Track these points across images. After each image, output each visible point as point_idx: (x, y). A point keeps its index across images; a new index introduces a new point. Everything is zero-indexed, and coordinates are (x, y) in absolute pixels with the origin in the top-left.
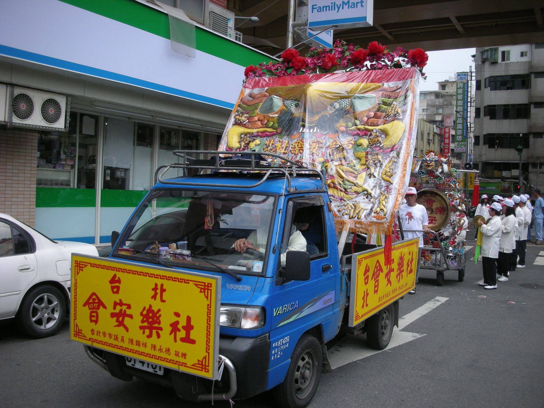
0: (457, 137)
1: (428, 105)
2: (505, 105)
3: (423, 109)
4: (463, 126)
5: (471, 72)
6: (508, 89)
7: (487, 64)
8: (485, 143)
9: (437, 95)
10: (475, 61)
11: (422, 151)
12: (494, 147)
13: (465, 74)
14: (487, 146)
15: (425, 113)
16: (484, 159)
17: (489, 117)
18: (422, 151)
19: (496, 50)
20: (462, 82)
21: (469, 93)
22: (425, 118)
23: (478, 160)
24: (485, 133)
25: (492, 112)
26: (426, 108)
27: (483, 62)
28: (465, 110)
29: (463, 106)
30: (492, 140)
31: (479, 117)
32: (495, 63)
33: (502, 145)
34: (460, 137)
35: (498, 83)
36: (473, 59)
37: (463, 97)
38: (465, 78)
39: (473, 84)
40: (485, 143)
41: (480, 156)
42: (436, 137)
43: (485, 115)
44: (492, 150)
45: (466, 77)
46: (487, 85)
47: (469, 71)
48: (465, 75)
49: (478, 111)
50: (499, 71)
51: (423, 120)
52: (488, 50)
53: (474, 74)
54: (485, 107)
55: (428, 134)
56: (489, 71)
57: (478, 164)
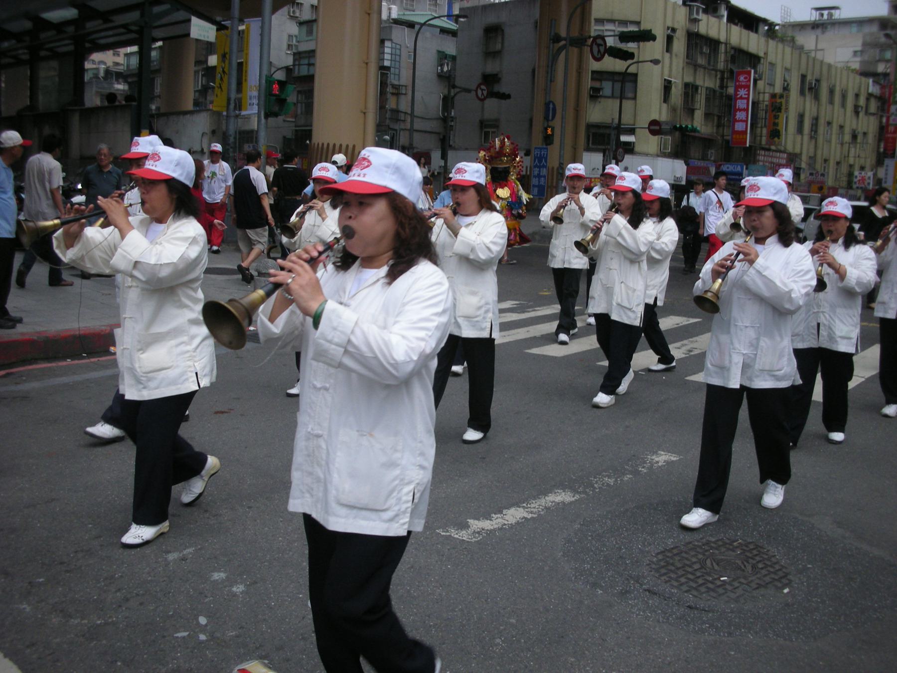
1: (865, 44)
3: (855, 52)
11: (841, 127)
15: (858, 59)
26: (859, 48)
51: (854, 71)
55: (857, 96)
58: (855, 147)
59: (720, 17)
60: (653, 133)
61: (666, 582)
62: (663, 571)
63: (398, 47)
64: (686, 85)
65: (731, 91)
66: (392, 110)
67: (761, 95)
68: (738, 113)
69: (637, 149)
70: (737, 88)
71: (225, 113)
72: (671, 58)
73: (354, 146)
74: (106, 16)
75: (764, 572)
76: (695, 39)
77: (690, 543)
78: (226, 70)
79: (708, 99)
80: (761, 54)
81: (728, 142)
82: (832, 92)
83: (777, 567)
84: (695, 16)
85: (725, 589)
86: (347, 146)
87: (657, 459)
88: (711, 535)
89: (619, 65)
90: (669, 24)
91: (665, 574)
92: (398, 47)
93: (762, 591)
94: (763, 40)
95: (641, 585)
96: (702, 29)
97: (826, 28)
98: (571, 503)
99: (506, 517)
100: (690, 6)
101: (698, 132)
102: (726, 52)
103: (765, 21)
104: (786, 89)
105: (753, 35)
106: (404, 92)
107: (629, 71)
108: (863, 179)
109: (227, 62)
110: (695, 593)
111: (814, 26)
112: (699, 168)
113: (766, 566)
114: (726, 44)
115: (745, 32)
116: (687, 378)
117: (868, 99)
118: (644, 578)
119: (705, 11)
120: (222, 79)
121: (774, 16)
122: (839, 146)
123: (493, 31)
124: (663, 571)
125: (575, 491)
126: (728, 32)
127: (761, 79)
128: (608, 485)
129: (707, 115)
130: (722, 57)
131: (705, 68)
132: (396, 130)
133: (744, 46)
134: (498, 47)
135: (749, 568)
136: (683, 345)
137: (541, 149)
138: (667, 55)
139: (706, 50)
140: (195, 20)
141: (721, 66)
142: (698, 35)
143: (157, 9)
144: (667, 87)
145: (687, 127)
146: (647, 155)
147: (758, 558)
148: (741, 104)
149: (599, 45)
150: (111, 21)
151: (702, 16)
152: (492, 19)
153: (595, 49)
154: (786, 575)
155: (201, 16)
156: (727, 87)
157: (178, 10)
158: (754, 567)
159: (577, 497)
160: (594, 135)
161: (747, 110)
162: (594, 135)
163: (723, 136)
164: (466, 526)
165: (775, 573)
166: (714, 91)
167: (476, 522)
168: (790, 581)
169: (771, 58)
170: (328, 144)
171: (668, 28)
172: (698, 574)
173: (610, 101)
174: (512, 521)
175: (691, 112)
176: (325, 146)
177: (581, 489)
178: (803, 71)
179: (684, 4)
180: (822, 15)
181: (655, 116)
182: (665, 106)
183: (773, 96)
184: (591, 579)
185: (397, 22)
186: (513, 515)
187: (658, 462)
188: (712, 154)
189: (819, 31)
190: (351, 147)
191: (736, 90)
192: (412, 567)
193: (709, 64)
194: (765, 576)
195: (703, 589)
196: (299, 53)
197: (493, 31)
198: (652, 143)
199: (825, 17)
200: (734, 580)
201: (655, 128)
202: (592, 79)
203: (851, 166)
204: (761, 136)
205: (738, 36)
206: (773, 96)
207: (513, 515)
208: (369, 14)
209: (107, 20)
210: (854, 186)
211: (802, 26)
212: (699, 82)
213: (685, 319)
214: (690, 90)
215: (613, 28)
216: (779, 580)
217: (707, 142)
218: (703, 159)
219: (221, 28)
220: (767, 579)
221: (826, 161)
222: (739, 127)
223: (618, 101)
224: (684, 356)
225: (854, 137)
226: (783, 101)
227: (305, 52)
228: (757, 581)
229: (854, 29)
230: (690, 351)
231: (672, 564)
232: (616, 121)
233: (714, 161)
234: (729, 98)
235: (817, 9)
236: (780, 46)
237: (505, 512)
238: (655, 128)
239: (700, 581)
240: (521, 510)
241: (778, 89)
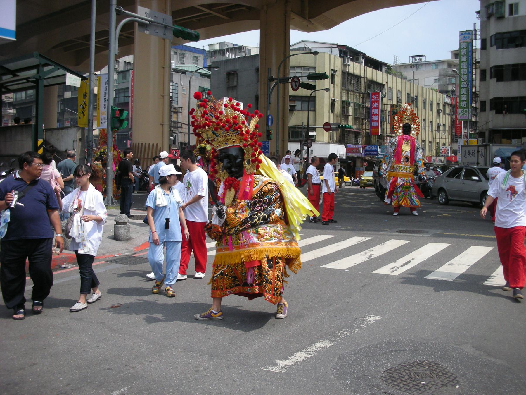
0: (462, 103)
1: (440, 75)
2: (513, 65)
3: (435, 80)
4: (468, 90)
5: (476, 31)
6: (517, 46)
7: (493, 20)
8: (491, 109)
9: (450, 64)
10: (480, 17)
11: (431, 122)
12: (502, 113)
13: (469, 32)
14: (494, 111)
15: (437, 84)
16: (491, 126)
17: (495, 79)
18: (431, 122)
19: (503, 3)
20: (465, 42)
21: (474, 54)
22: (437, 88)
23: (484, 129)
24: (492, 97)
25: (499, 73)
26: (438, 78)
27: (489, 17)
28: (470, 73)
29: (468, 68)
30: (500, 105)
31: (485, 80)
32: (501, 17)
33: (510, 111)
34: (465, 103)
35: (506, 40)
36: (478, 15)
37: (468, 58)
38: (469, 37)
39: (477, 44)
40: (491, 109)
41: (487, 123)
42: (447, 106)
43: (491, 78)
44: (500, 116)
45: (470, 36)
46: (493, 43)
47: (473, 30)
48: (469, 34)
49: (483, 73)
50: (507, 26)
52: (493, 4)
53: (478, 33)
54: (491, 68)
55: (438, 104)
56: (495, 28)
57: (484, 133)
58: (439, 133)
59: (360, 63)
60: (326, 130)
61: (393, 387)
62: (389, 381)
63: (177, 85)
64: (343, 102)
65: (368, 105)
66: (174, 122)
67: (386, 106)
68: (373, 116)
69: (317, 139)
70: (372, 103)
71: (87, 128)
72: (334, 87)
73: (157, 144)
74: (14, 73)
75: (443, 377)
76: (346, 75)
77: (400, 364)
78: (87, 103)
79: (356, 110)
80: (384, 83)
81: (368, 133)
82: (424, 103)
83: (449, 374)
84: (346, 63)
85: (425, 388)
86: (153, 144)
87: (369, 319)
88: (410, 360)
89: (305, 92)
90: (332, 68)
91: (391, 383)
92: (177, 85)
93: (445, 388)
94: (385, 75)
95: (380, 390)
96: (351, 70)
97: (419, 67)
98: (330, 347)
99: (297, 358)
100: (343, 57)
101: (352, 128)
102: (365, 82)
103: (385, 64)
104: (399, 101)
105: (379, 72)
106: (180, 110)
107: (312, 95)
108: (445, 150)
109: (87, 98)
110: (410, 392)
111: (412, 66)
112: (353, 149)
113: (444, 374)
114: (364, 78)
115: (375, 71)
116: (373, 272)
117: (444, 106)
118: (381, 386)
119: (352, 60)
120: (83, 108)
121: (390, 62)
122: (430, 133)
123: (231, 75)
124: (389, 381)
125: (330, 341)
126: (366, 71)
127: (385, 97)
128: (347, 336)
129: (356, 119)
130: (362, 85)
131: (353, 92)
132: (177, 133)
133: (375, 79)
134: (235, 83)
135: (435, 376)
136: (366, 253)
137: (265, 142)
138: (332, 85)
139: (353, 82)
140: (69, 75)
141: (362, 90)
142: (349, 74)
143: (46, 69)
144: (333, 104)
145: (345, 126)
146: (323, 143)
147: (438, 370)
148: (375, 111)
149: (295, 82)
150: (18, 76)
151: (350, 63)
152: (231, 68)
153: (293, 83)
154: (455, 378)
155: (72, 72)
156: (366, 102)
157: (59, 69)
158: (437, 375)
159: (332, 344)
160: (292, 132)
161: (378, 115)
162: (292, 132)
163: (365, 130)
164: (276, 365)
165: (449, 377)
166: (359, 105)
167: (281, 362)
168: (458, 381)
169: (390, 85)
170: (142, 144)
171: (332, 70)
172: (409, 381)
173: (301, 112)
174: (301, 359)
175: (346, 117)
176: (140, 145)
177: (333, 339)
178: (408, 92)
179: (340, 56)
180: (416, 60)
181: (326, 120)
182: (332, 115)
183: (392, 106)
184: (353, 389)
185: (176, 71)
186: (300, 356)
187: (370, 321)
188: (361, 141)
189: (414, 69)
190: (155, 145)
191: (372, 104)
192: (253, 390)
193: (355, 90)
194: (444, 379)
195: (413, 389)
196: (119, 90)
197: (231, 75)
198: (326, 136)
199: (418, 61)
200: (428, 383)
201: (327, 127)
202: (290, 100)
203: (437, 143)
204: (387, 129)
205: (371, 73)
206: (392, 106)
207: (300, 356)
208: (164, 68)
209: (15, 75)
210: (440, 155)
211: (405, 66)
212: (350, 101)
213: (363, 238)
214: (345, 104)
215: (301, 71)
216: (452, 381)
217: (357, 134)
218: (355, 144)
219: (83, 79)
220: (446, 381)
221: (424, 141)
222: (374, 124)
223: (306, 113)
224: (368, 259)
225: (438, 127)
226: (398, 108)
227: (122, 89)
228: (441, 383)
229: (434, 67)
230: (371, 256)
231: (394, 377)
232: (306, 124)
233: (361, 145)
234: (367, 108)
235: (413, 57)
236: (395, 78)
237: (295, 354)
238: (327, 127)
239: (411, 385)
240: (303, 353)
241: (395, 102)
